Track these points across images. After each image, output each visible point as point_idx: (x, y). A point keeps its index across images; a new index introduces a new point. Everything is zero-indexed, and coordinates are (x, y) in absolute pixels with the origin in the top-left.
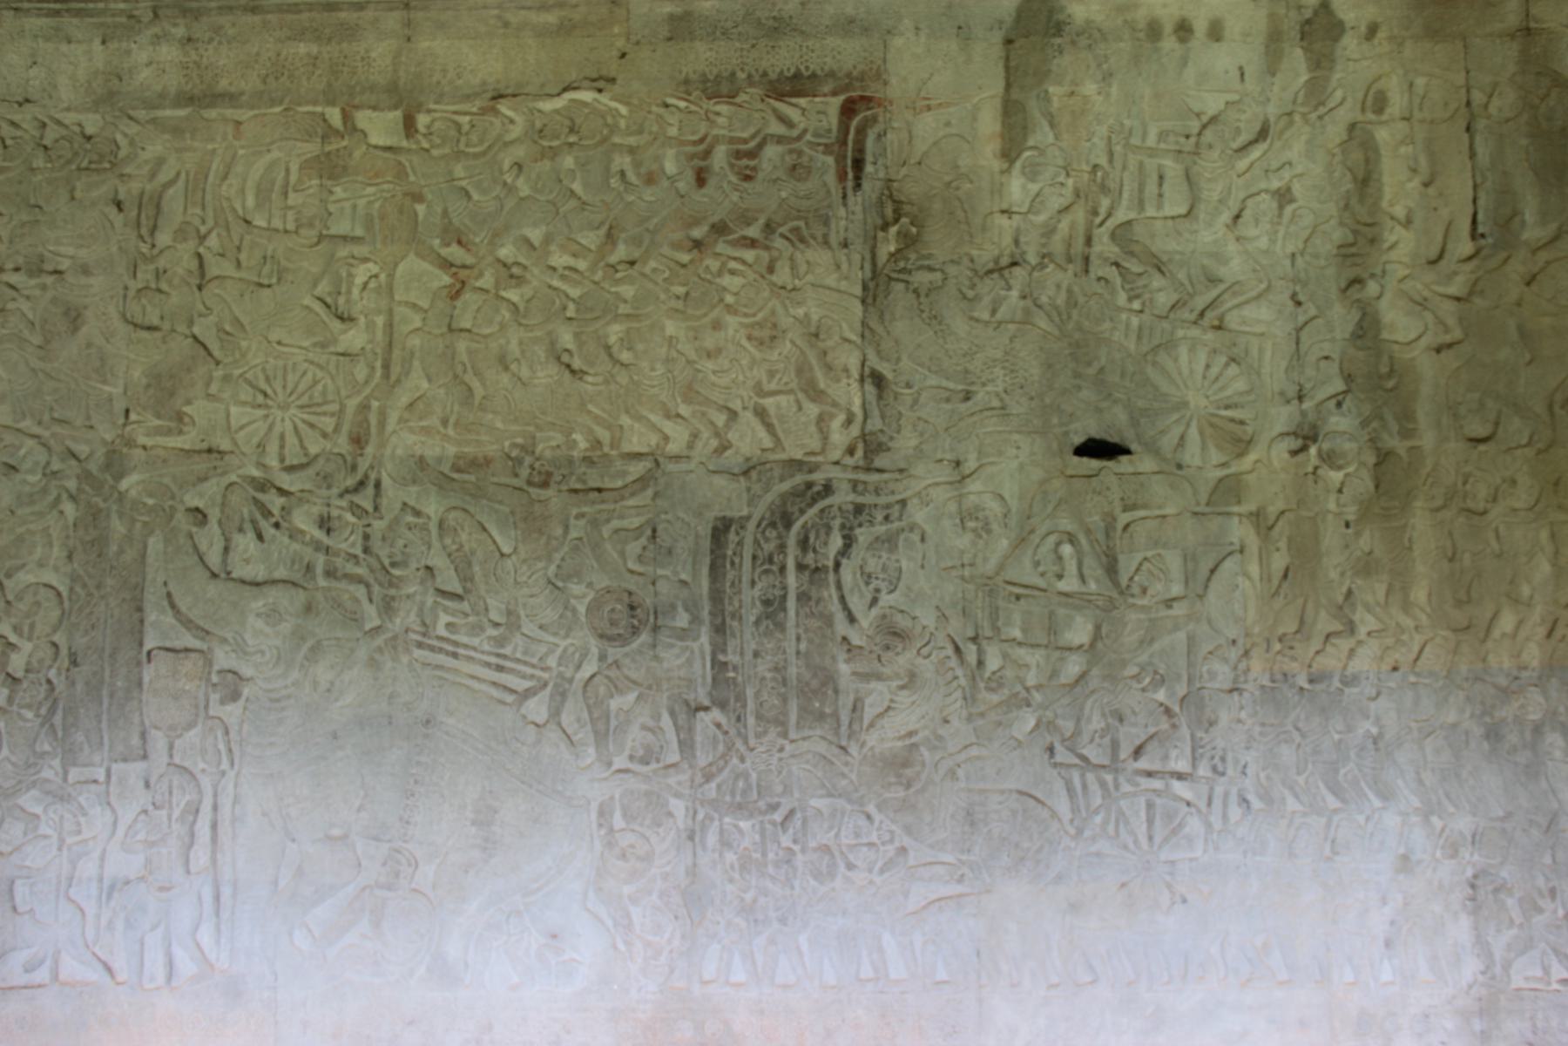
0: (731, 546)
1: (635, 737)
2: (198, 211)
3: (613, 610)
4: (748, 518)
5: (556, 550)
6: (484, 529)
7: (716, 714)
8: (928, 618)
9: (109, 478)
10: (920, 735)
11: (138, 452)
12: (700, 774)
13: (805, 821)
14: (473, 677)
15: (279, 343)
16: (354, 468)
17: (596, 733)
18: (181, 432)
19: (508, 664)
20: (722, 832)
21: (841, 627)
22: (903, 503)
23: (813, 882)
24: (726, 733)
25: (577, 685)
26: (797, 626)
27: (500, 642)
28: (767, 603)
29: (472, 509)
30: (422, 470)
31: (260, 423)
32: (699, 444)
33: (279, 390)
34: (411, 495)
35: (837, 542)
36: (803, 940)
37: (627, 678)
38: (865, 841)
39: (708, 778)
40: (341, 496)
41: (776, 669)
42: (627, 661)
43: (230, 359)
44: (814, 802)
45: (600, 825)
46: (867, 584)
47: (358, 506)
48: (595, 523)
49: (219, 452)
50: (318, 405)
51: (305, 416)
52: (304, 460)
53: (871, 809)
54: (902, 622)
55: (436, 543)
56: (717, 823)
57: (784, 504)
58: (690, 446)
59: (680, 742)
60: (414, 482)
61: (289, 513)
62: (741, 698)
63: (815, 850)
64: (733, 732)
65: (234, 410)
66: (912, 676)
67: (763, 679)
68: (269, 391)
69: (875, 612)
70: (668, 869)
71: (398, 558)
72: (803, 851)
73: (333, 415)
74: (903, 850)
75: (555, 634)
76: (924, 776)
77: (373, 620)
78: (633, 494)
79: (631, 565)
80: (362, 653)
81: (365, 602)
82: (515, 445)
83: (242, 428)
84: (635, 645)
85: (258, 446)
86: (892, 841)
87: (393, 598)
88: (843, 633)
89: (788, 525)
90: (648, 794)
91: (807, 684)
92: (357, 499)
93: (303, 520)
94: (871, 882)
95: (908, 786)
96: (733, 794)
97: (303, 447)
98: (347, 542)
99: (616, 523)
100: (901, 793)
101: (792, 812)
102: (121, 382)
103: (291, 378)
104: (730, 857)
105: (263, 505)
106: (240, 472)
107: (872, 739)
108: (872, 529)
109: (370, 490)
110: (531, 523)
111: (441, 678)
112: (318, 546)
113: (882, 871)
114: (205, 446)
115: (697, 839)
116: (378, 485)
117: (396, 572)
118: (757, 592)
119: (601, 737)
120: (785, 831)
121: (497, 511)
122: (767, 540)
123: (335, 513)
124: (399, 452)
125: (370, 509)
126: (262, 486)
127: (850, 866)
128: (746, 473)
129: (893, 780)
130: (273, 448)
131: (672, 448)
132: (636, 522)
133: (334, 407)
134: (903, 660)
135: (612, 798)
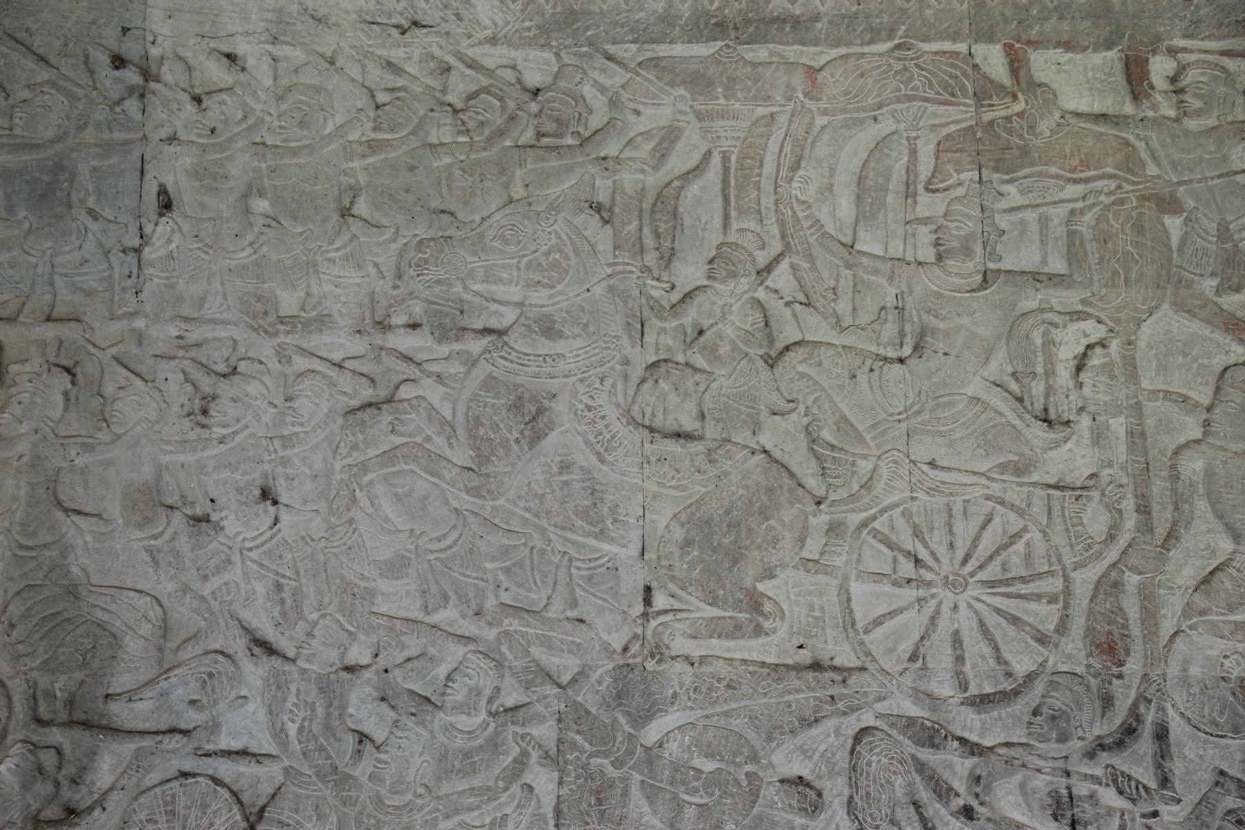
2: (752, 225)
9: (622, 720)
11: (679, 666)
15: (932, 464)
16: (1107, 702)
18: (758, 631)
31: (911, 613)
33: (942, 551)
40: (1091, 755)
43: (843, 493)
49: (835, 669)
50: (1022, 579)
51: (999, 602)
52: (1007, 686)
61: (988, 788)
65: (856, 588)
68: (923, 554)
73: (1052, 600)
83: (878, 622)
85: (913, 657)
92: (1120, 761)
97: (1000, 660)
102: (634, 536)
103: (964, 531)
106: (881, 707)
109: (1145, 745)
114: (805, 657)
116: (1161, 735)
123: (1082, 789)
126: (932, 737)
130: (941, 659)
133: (1056, 584)
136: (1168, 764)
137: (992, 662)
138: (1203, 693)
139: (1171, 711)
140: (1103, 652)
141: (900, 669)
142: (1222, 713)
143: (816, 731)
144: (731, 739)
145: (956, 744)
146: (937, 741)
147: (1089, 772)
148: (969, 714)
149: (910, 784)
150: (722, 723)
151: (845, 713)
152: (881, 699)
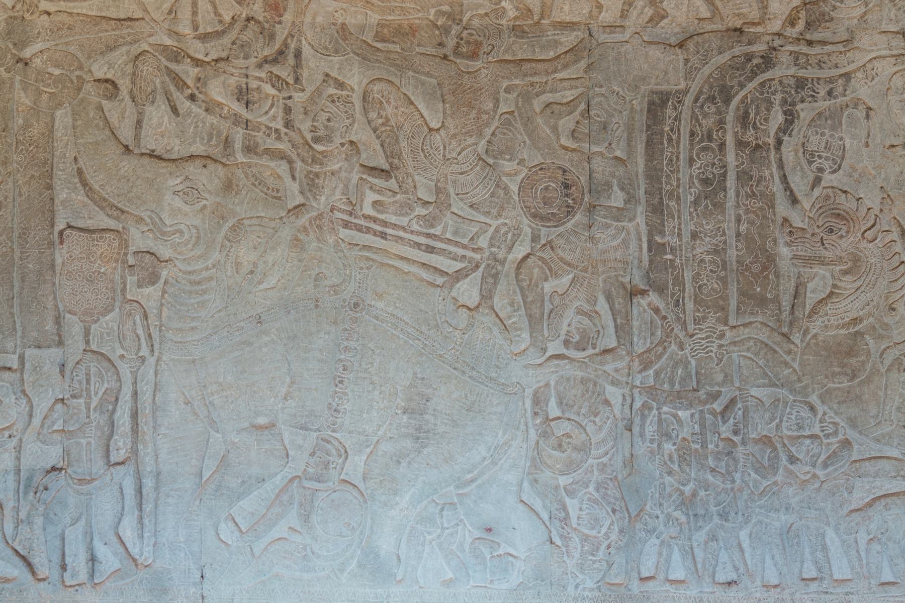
0: (669, 122)
1: (570, 321)
3: (546, 188)
4: (686, 91)
5: (487, 125)
6: (412, 103)
7: (653, 298)
8: (872, 200)
10: (865, 323)
12: (637, 363)
13: (746, 411)
14: (402, 258)
16: (272, 37)
17: (530, 316)
19: (439, 245)
20: (660, 421)
21: (782, 208)
22: (847, 76)
23: (753, 475)
24: (665, 318)
25: (509, 268)
26: (738, 206)
27: (430, 221)
28: (706, 182)
29: (397, 81)
30: (345, 40)
32: (634, 13)
34: (333, 65)
35: (778, 118)
36: (744, 535)
37: (561, 259)
38: (807, 433)
39: (646, 366)
40: (260, 66)
41: (716, 252)
42: (561, 242)
44: (754, 392)
45: (536, 414)
46: (810, 163)
47: (278, 77)
48: (526, 97)
53: (814, 399)
54: (846, 204)
55: (358, 115)
56: (655, 412)
57: (723, 77)
58: (624, 15)
59: (616, 327)
60: (337, 52)
61: (205, 84)
62: (679, 281)
63: (756, 441)
64: (671, 317)
66: (856, 260)
67: (702, 261)
69: (817, 192)
70: (605, 460)
71: (321, 133)
72: (744, 443)
74: (846, 444)
75: (487, 214)
76: (869, 366)
77: (294, 194)
78: (566, 67)
79: (564, 141)
80: (286, 233)
81: (288, 179)
82: (441, 13)
84: (569, 225)
85: (170, 12)
86: (836, 433)
87: (317, 175)
88: (784, 214)
89: (727, 101)
90: (583, 381)
91: (748, 268)
92: (276, 70)
93: (217, 91)
94: (815, 476)
95: (854, 377)
96: (672, 382)
97: (217, 14)
98: (268, 115)
99: (547, 97)
100: (847, 384)
101: (733, 401)
104: (668, 447)
105: (177, 75)
106: (151, 40)
107: (815, 327)
108: (816, 104)
110: (459, 97)
111: (368, 259)
112: (236, 120)
113: (825, 465)
115: (636, 429)
116: (298, 55)
117: (319, 147)
118: (695, 171)
119: (534, 323)
120: (724, 422)
121: (423, 84)
122: (705, 115)
123: (254, 84)
124: (319, 19)
125: (291, 81)
126: (176, 56)
127: (793, 460)
128: (681, 45)
129: (837, 370)
130: (185, 14)
131: (606, 17)
132: (569, 95)
134: (844, 245)
135: (547, 385)
136: (300, 71)
137: (212, 15)
138: (322, 31)
139: (304, 42)
140: (272, 9)
141: (162, 18)
142: (330, 42)
143: (116, 53)
144: (68, 57)
145: (189, 60)
146: (179, 58)
147: (258, 75)
148: (198, 44)
149: (163, 82)
150: (64, 49)
151: (131, 43)
152: (151, 35)
